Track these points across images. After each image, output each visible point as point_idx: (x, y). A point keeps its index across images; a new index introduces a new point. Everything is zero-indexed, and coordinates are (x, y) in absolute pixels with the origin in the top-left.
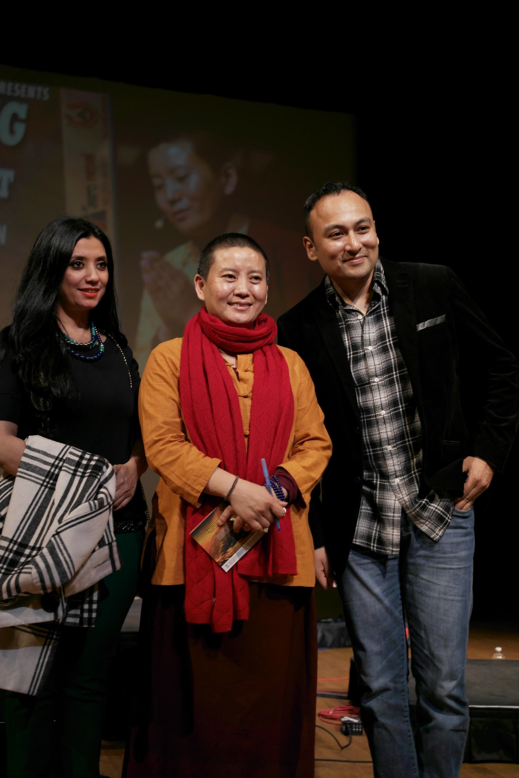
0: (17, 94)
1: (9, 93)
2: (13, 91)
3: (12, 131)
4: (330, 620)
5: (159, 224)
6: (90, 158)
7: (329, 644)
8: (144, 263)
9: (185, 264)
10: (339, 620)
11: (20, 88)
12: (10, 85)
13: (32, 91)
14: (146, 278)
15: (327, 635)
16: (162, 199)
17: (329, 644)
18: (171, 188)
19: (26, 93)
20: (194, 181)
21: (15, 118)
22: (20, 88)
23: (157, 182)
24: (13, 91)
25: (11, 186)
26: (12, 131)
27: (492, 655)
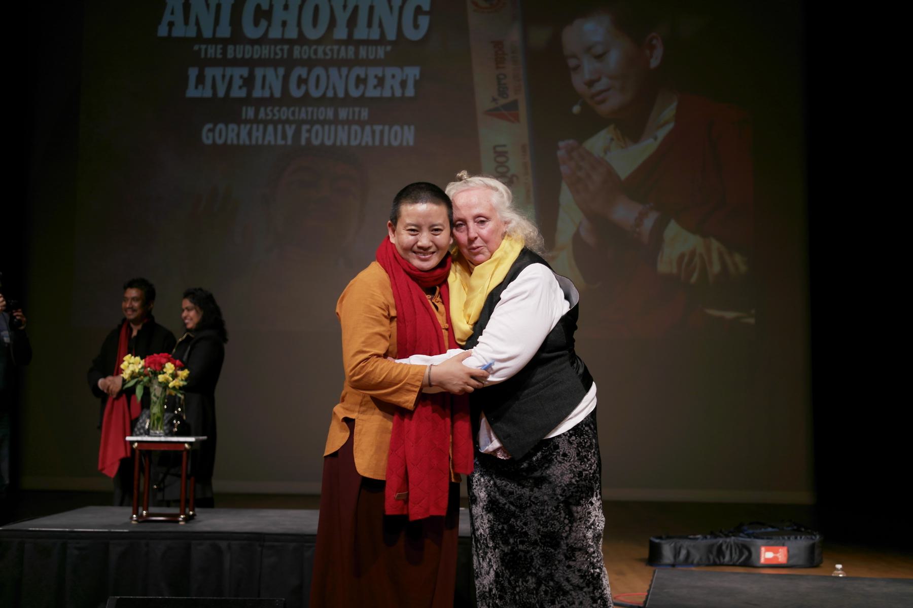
3: (416, 26)
4: (698, 536)
5: (576, 109)
6: (498, 45)
7: (695, 562)
8: (561, 153)
9: (606, 150)
10: (709, 537)
14: (564, 169)
15: (693, 551)
16: (578, 81)
17: (695, 562)
18: (589, 68)
20: (614, 58)
21: (418, 10)
23: (572, 63)
25: (416, 83)
26: (416, 26)
27: (832, 572)
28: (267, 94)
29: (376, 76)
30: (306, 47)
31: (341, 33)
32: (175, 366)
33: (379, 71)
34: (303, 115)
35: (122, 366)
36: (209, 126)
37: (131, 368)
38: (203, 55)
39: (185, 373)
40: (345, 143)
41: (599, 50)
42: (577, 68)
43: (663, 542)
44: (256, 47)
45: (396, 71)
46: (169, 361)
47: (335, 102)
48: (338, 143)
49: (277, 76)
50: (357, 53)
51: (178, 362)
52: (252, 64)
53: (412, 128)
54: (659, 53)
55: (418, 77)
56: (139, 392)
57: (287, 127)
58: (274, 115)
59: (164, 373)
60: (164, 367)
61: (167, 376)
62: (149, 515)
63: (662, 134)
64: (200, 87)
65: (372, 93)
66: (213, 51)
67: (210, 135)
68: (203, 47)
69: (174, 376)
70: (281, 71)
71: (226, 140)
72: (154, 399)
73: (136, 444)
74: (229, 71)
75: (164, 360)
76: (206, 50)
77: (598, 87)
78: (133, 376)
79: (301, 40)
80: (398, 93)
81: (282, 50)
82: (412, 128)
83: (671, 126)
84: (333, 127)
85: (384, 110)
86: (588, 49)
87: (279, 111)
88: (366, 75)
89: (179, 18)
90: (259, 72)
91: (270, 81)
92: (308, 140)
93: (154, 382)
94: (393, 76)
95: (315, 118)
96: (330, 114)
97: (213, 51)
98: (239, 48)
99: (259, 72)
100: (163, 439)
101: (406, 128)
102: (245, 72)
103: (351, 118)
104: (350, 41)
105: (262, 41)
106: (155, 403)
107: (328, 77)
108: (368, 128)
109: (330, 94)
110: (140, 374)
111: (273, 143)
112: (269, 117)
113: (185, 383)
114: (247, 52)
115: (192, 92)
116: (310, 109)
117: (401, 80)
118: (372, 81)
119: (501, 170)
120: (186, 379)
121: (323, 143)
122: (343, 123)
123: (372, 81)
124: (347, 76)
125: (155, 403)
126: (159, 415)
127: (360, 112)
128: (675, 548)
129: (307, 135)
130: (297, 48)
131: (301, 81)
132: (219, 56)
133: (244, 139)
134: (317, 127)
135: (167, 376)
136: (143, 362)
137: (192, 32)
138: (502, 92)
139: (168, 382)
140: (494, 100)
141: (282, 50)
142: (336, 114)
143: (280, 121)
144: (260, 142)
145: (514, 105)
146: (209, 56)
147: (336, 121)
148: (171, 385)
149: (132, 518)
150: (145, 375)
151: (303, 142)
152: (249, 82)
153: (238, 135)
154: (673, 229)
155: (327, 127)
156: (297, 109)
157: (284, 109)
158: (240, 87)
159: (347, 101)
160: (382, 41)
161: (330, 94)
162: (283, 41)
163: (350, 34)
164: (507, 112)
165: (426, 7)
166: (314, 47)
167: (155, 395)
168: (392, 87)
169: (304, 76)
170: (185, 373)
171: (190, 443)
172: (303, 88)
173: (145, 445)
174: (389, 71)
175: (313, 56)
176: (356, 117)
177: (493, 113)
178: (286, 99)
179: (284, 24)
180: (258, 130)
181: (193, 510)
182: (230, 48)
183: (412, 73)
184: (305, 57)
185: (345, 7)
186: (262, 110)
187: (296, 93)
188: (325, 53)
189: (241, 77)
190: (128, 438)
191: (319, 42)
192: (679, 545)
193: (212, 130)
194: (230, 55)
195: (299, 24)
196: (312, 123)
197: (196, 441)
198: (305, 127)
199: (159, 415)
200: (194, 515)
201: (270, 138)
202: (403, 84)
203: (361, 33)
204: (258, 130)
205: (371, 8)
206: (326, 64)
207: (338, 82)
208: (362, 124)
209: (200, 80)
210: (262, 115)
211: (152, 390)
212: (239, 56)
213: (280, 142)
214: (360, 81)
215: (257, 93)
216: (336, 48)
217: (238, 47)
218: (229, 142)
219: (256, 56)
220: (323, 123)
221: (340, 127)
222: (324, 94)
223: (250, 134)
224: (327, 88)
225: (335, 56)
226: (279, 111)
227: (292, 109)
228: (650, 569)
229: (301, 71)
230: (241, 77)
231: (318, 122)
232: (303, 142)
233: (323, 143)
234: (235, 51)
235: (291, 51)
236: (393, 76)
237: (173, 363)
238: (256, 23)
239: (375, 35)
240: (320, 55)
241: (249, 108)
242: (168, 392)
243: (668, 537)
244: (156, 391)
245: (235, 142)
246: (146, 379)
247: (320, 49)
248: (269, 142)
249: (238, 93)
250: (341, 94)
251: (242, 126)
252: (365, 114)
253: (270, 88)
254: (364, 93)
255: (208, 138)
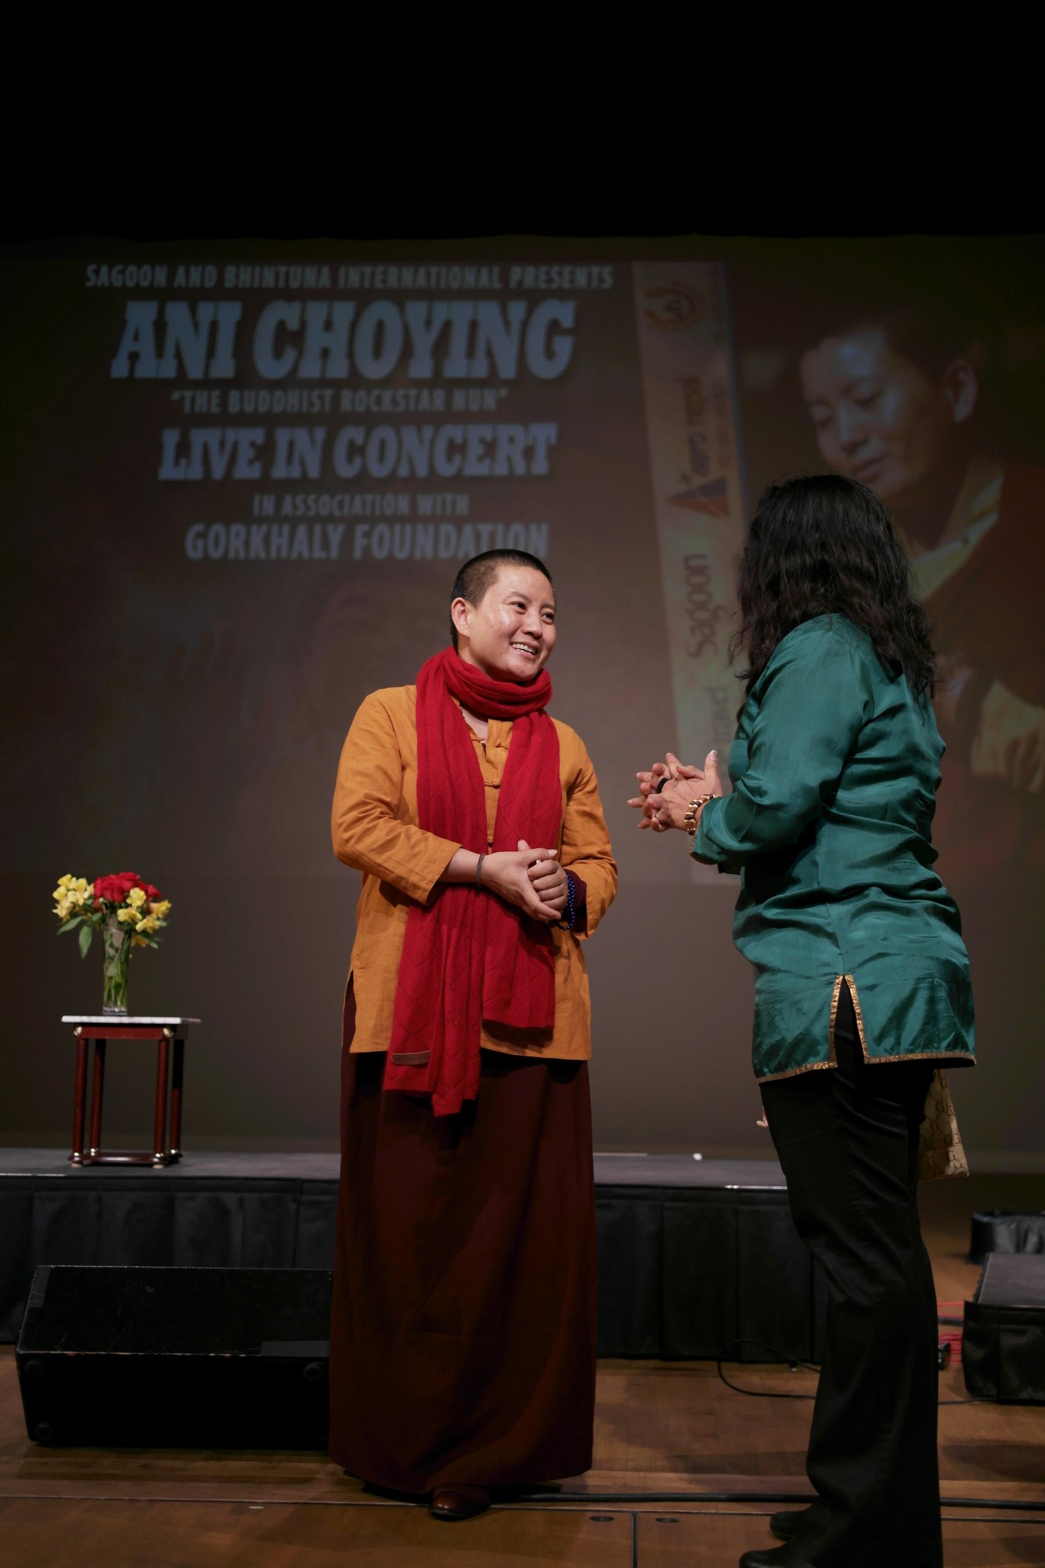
0: (554, 286)
1: (543, 286)
2: (550, 280)
3: (550, 354)
11: (560, 274)
12: (543, 269)
13: (581, 277)
18: (848, 421)
19: (572, 281)
20: (892, 404)
21: (554, 328)
22: (560, 274)
23: (819, 413)
24: (550, 280)
25: (552, 452)
26: (550, 354)
28: (296, 473)
29: (482, 441)
30: (362, 393)
31: (422, 367)
32: (146, 893)
33: (486, 431)
34: (357, 509)
35: (56, 895)
36: (198, 528)
37: (72, 897)
38: (187, 409)
39: (162, 907)
40: (429, 555)
41: (865, 390)
42: (828, 422)
43: (996, 1221)
44: (278, 394)
45: (516, 430)
46: (136, 884)
47: (412, 485)
48: (418, 555)
49: (313, 442)
50: (448, 401)
51: (151, 889)
52: (269, 421)
53: (545, 527)
54: (969, 394)
55: (553, 442)
56: (85, 940)
57: (330, 528)
58: (308, 508)
59: (128, 906)
60: (128, 896)
61: (133, 911)
62: (98, 1154)
63: (976, 533)
64: (183, 462)
65: (475, 468)
66: (205, 402)
67: (200, 543)
68: (188, 394)
69: (145, 912)
70: (320, 434)
71: (226, 552)
72: (110, 951)
73: (79, 1030)
74: (231, 435)
75: (127, 884)
76: (193, 400)
77: (865, 454)
78: (73, 913)
79: (355, 380)
80: (520, 469)
81: (322, 398)
82: (545, 527)
83: (991, 520)
84: (408, 528)
85: (495, 498)
86: (847, 390)
87: (316, 501)
88: (465, 441)
89: (147, 345)
90: (283, 436)
91: (302, 450)
92: (367, 550)
93: (111, 921)
94: (511, 440)
95: (377, 512)
96: (403, 505)
97: (205, 402)
98: (249, 395)
99: (283, 436)
100: (126, 1020)
101: (533, 527)
102: (258, 435)
103: (438, 511)
104: (437, 381)
105: (290, 381)
106: (112, 959)
107: (400, 442)
108: (468, 530)
109: (403, 471)
110: (87, 908)
111: (306, 555)
112: (300, 512)
113: (164, 924)
114: (261, 401)
115: (169, 471)
116: (369, 497)
117: (525, 447)
118: (475, 449)
119: (699, 597)
120: (167, 917)
121: (391, 557)
122: (426, 520)
123: (475, 449)
124: (432, 442)
125: (112, 959)
126: (119, 979)
127: (454, 503)
128: (1017, 1231)
129: (365, 542)
130: (346, 395)
131: (355, 450)
132: (215, 410)
133: (256, 549)
134: (382, 528)
135: (133, 911)
136: (91, 889)
137: (168, 370)
138: (699, 463)
139: (134, 922)
140: (685, 478)
141: (322, 398)
142: (414, 505)
143: (318, 518)
144: (284, 554)
145: (718, 487)
146: (197, 409)
147: (413, 518)
148: (139, 927)
149: (72, 1158)
150: (96, 910)
151: (358, 554)
152: (265, 453)
153: (247, 543)
154: (998, 696)
155: (397, 528)
156: (347, 498)
157: (325, 498)
158: (251, 462)
159: (433, 483)
160: (492, 380)
161: (403, 471)
162: (323, 383)
163: (438, 369)
164: (707, 498)
165: (567, 320)
166: (376, 392)
167: (112, 945)
168: (509, 459)
169: (359, 441)
170: (162, 907)
171: (172, 1027)
172: (358, 461)
173: (95, 1029)
174: (505, 431)
175: (374, 408)
176: (449, 510)
177: (684, 500)
178: (329, 481)
179: (325, 353)
180: (280, 534)
181: (177, 1148)
182: (234, 396)
183: (545, 433)
184: (361, 409)
185: (428, 323)
186: (288, 500)
187: (345, 470)
188: (395, 403)
189: (253, 444)
190: (66, 1019)
191: (384, 383)
192: (1024, 1226)
193: (203, 535)
194: (234, 407)
195: (351, 354)
196: (373, 520)
197: (183, 1026)
198: (361, 529)
199: (119, 979)
200: (178, 1156)
201: (301, 548)
202: (529, 453)
203: (456, 367)
204: (280, 534)
205: (474, 326)
206: (397, 420)
207: (417, 450)
208: (458, 522)
209: (183, 449)
210: (287, 508)
211: (106, 936)
212: (249, 409)
213: (319, 554)
214: (455, 449)
215: (280, 471)
216: (413, 392)
217: (246, 393)
218: (232, 555)
219: (277, 409)
220: (391, 520)
221: (420, 528)
222: (394, 472)
223: (267, 541)
224: (398, 461)
225: (412, 408)
226: (316, 501)
227: (338, 498)
228: (972, 1267)
229: (354, 433)
230: (253, 444)
231: (384, 519)
232: (358, 554)
233: (391, 557)
234: (242, 400)
235: (336, 400)
236: (511, 440)
237: (142, 889)
238: (278, 353)
239: (480, 370)
240: (387, 405)
241: (266, 498)
242: (133, 943)
243: (1006, 1213)
244: (115, 937)
245: (242, 555)
246: (96, 917)
247: (387, 395)
248: (300, 554)
249: (247, 471)
250: (422, 471)
251: (254, 528)
252: (463, 504)
253: (302, 463)
254: (460, 471)
255: (195, 548)
